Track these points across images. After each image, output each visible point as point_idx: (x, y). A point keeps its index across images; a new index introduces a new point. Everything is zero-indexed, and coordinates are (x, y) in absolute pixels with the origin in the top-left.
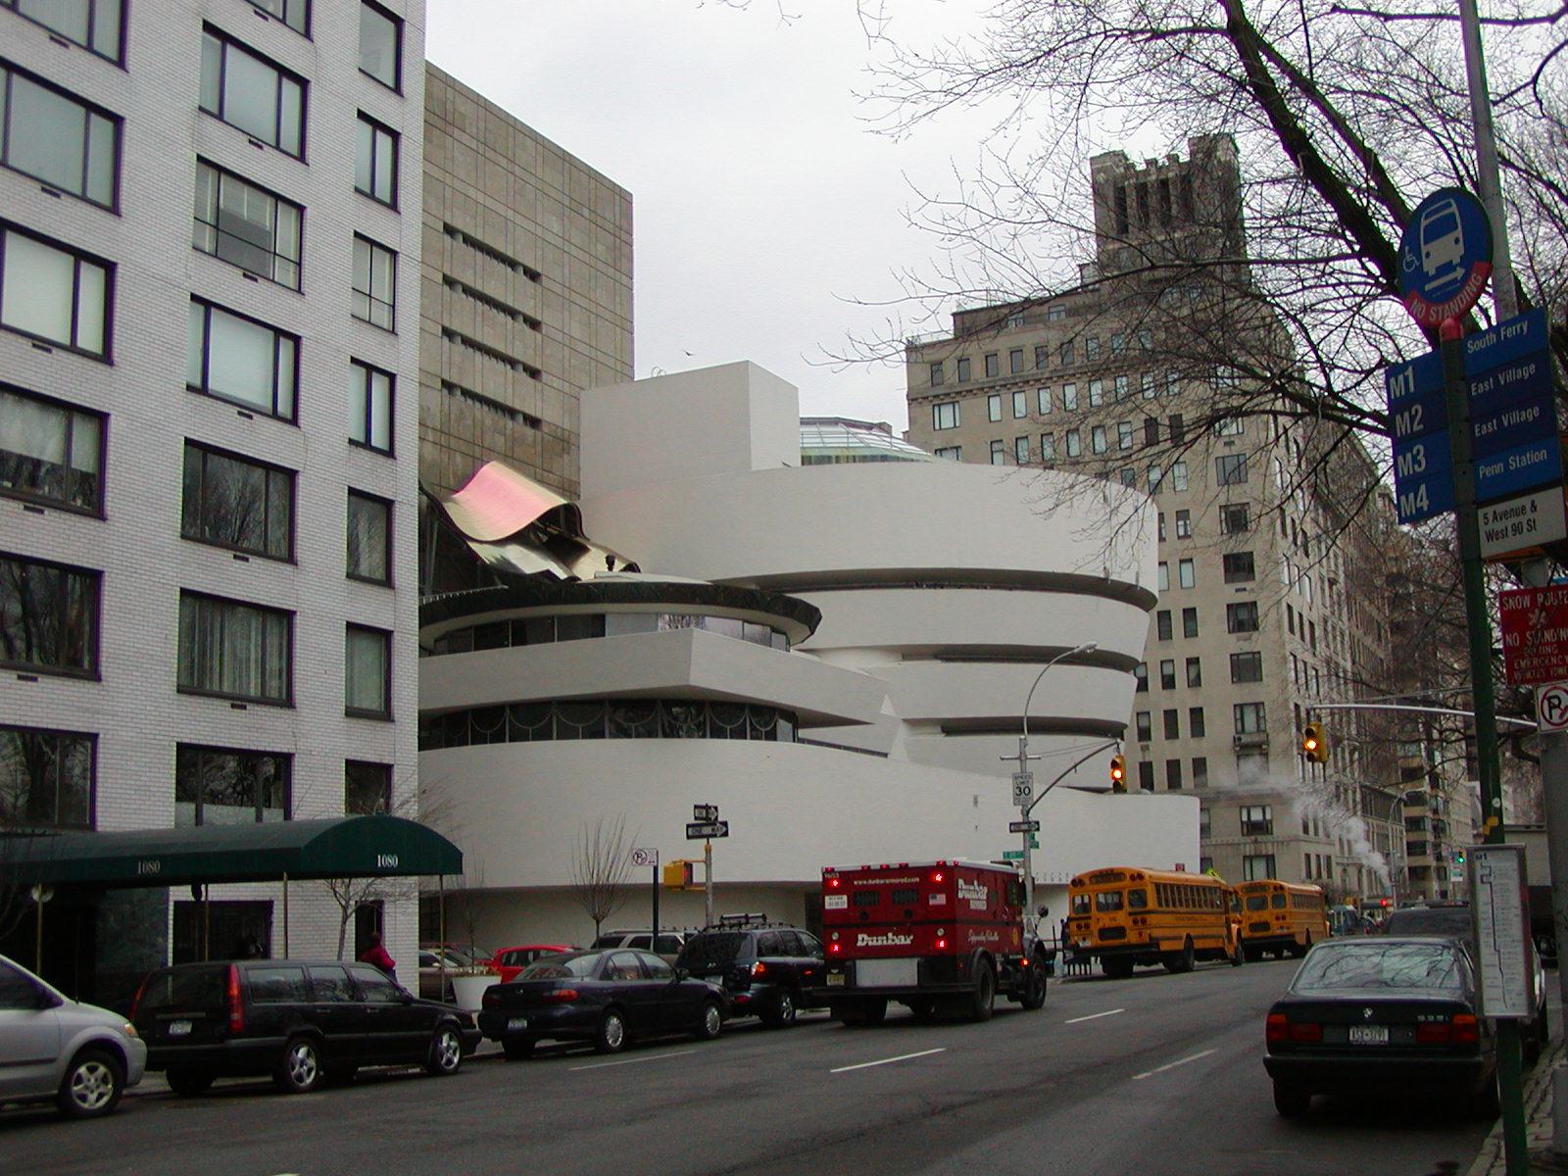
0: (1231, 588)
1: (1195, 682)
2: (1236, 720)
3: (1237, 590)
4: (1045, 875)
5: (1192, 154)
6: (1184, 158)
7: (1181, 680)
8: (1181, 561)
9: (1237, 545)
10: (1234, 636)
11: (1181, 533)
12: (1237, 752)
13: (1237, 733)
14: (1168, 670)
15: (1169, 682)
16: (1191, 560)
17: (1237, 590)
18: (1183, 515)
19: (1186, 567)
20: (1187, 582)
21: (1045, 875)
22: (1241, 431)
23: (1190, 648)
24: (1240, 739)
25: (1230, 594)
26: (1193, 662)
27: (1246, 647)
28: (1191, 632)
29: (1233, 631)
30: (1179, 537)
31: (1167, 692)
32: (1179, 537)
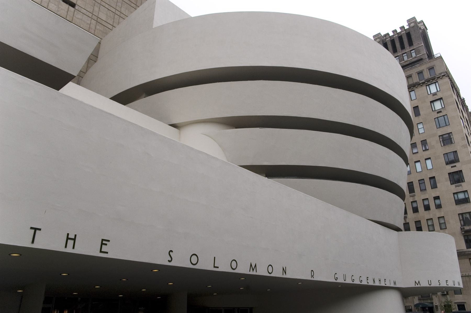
0: (449, 167)
1: (439, 207)
2: (460, 220)
3: (452, 167)
4: (345, 276)
5: (409, 25)
6: (406, 27)
7: (432, 206)
8: (426, 159)
9: (449, 149)
10: (454, 186)
11: (424, 149)
12: (463, 234)
13: (462, 226)
14: (426, 203)
15: (427, 208)
16: (430, 158)
17: (452, 167)
18: (424, 143)
19: (429, 162)
20: (429, 166)
21: (345, 276)
22: (443, 107)
23: (435, 193)
24: (464, 228)
25: (449, 169)
26: (437, 198)
27: (460, 189)
28: (434, 186)
29: (453, 184)
30: (424, 151)
31: (427, 212)
32: (424, 151)
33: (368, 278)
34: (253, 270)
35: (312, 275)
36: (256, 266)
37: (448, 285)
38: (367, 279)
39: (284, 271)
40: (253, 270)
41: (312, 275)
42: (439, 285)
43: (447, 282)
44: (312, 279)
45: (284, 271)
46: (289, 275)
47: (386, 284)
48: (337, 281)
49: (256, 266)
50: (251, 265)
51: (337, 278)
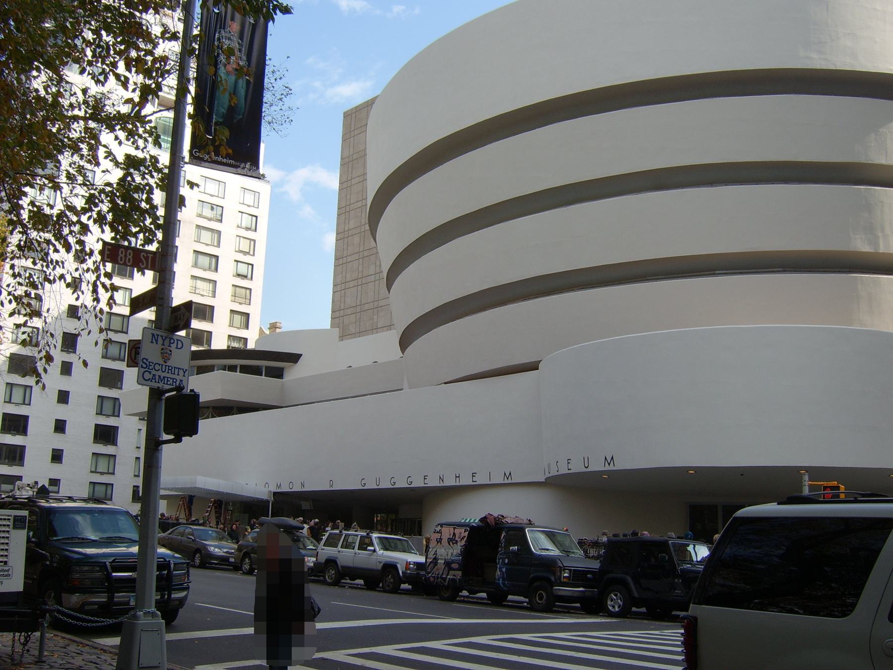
33: (425, 477)
34: (279, 488)
35: (331, 485)
36: (280, 485)
37: (571, 469)
38: (425, 479)
39: (302, 485)
40: (279, 488)
41: (331, 485)
42: (558, 471)
43: (569, 463)
44: (331, 489)
45: (302, 485)
46: (307, 488)
47: (473, 481)
48: (364, 488)
49: (280, 485)
50: (277, 485)
51: (365, 484)
